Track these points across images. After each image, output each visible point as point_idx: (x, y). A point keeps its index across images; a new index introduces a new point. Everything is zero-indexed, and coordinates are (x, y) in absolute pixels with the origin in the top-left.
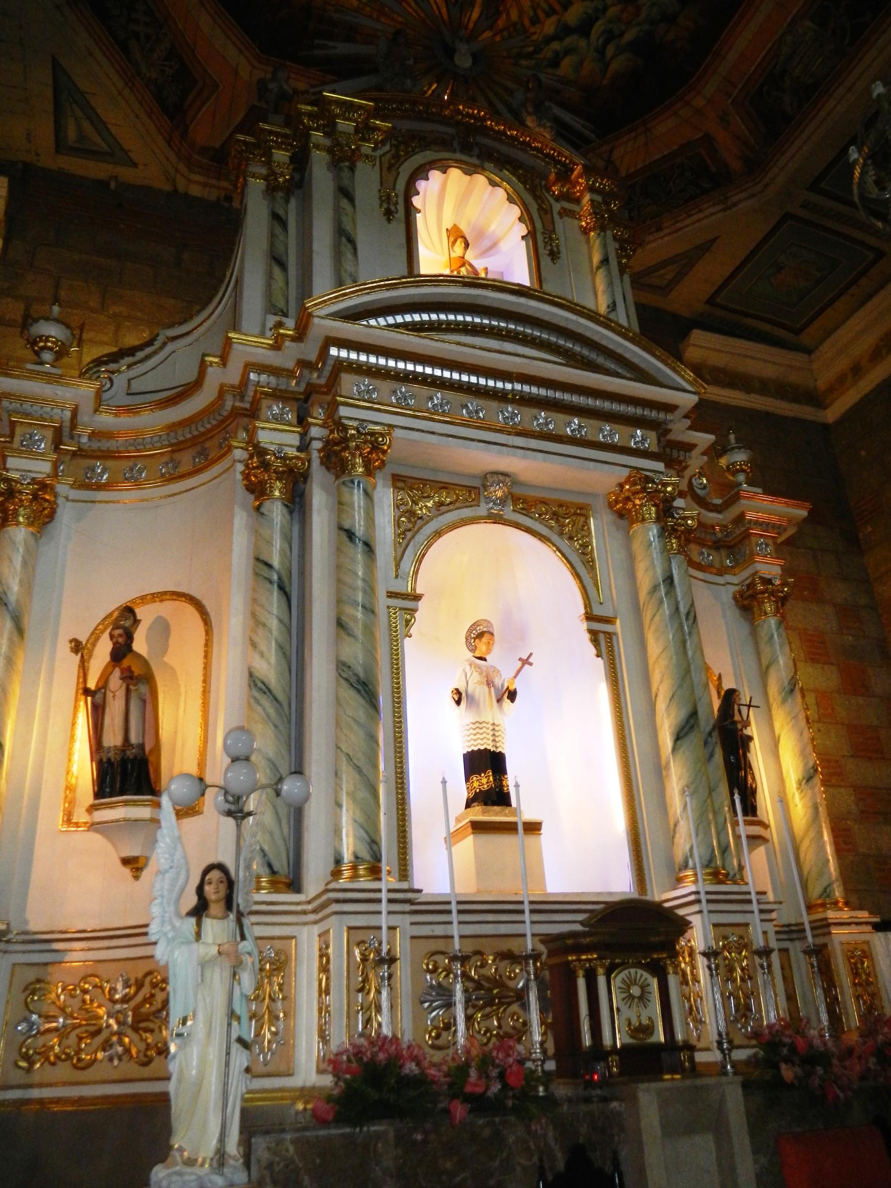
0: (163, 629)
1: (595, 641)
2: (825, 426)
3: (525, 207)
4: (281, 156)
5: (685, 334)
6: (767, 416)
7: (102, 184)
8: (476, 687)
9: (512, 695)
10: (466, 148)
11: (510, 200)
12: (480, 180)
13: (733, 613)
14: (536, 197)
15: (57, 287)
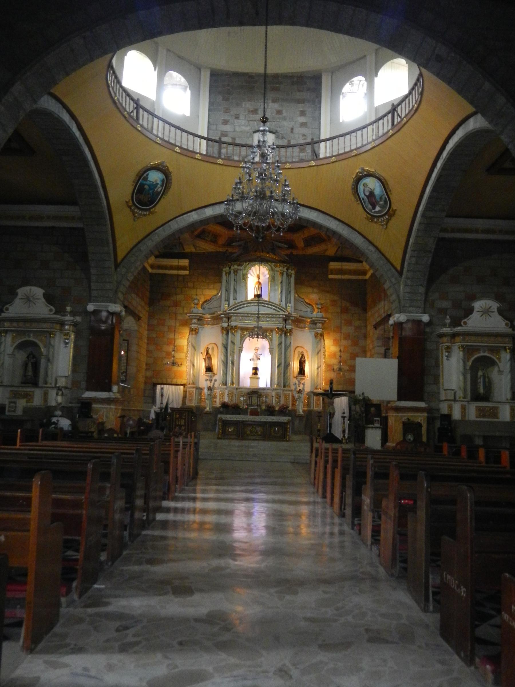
0: (213, 348)
1: (270, 352)
2: (365, 280)
3: (269, 270)
4: (228, 268)
5: (329, 263)
6: (349, 280)
7: (204, 253)
8: (255, 358)
9: (259, 359)
10: (259, 261)
11: (266, 270)
12: (261, 267)
13: (314, 337)
14: (272, 268)
15: (198, 279)
